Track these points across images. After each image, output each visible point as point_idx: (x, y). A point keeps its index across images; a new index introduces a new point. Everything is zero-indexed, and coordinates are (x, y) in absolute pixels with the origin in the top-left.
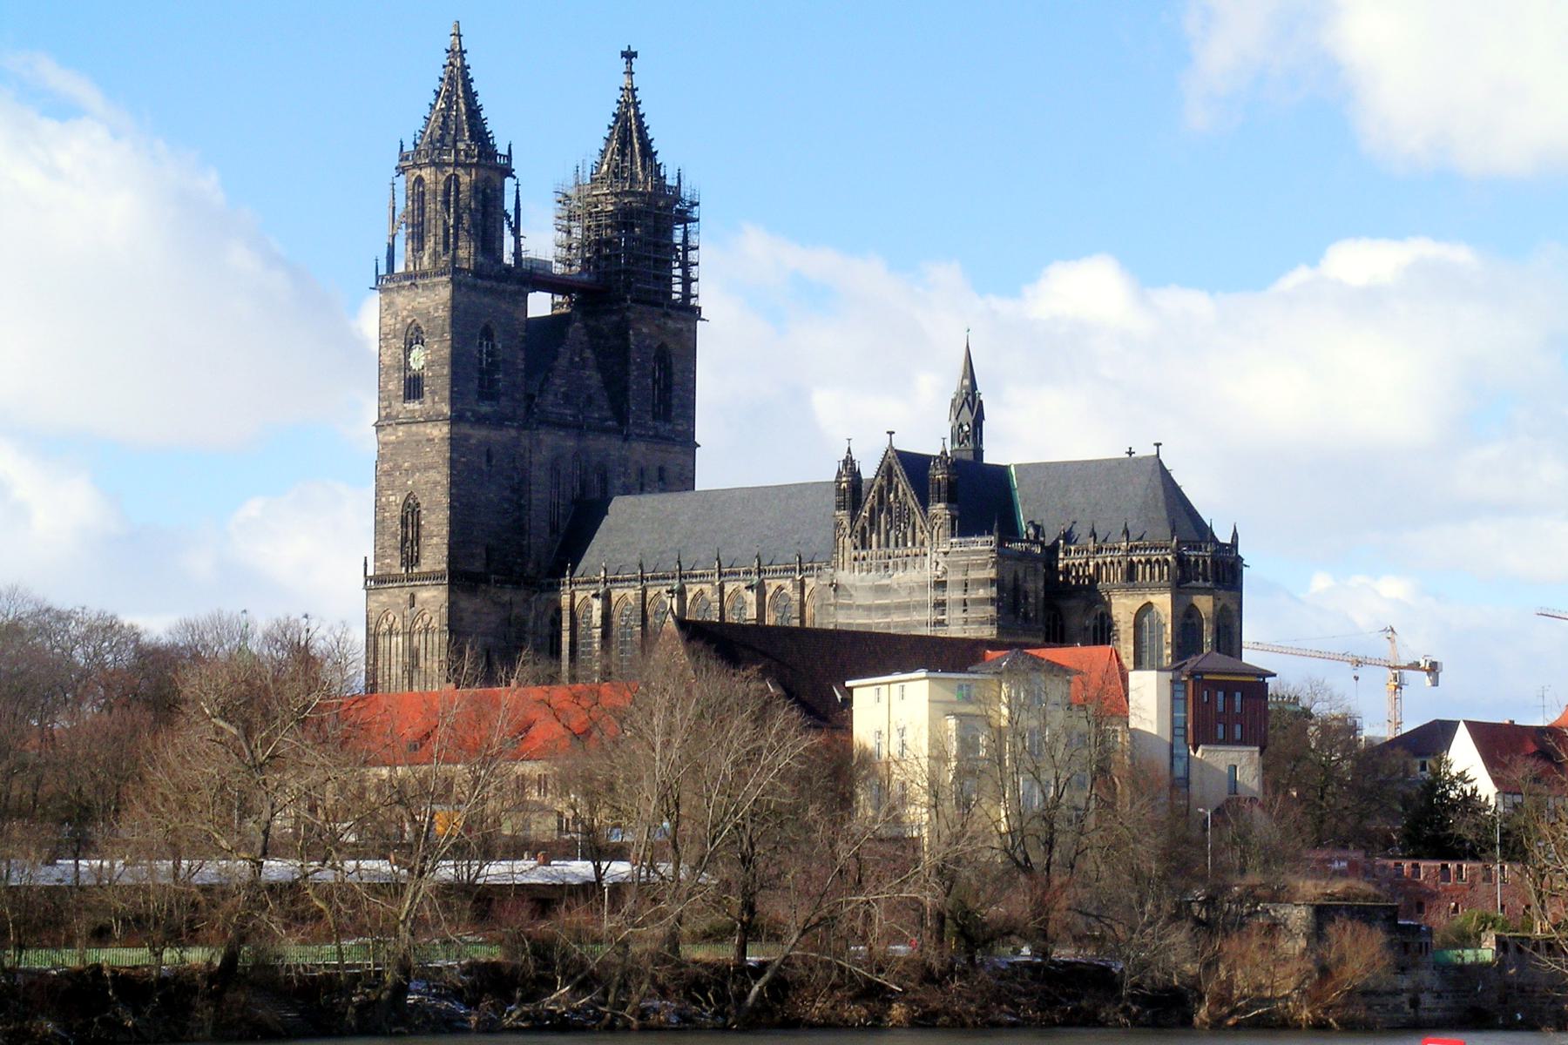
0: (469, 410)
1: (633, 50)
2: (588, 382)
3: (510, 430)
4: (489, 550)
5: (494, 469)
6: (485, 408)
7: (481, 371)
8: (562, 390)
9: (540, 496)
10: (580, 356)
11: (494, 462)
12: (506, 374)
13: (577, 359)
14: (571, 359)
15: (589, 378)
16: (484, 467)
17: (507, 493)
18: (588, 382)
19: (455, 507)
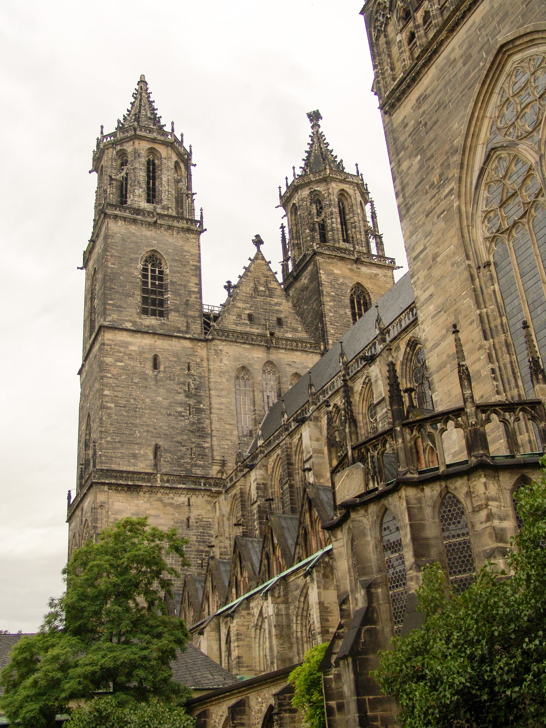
0: (130, 321)
1: (315, 109)
2: (277, 308)
3: (182, 341)
4: (157, 448)
5: (162, 375)
6: (151, 321)
7: (145, 291)
8: (247, 312)
9: (223, 400)
10: (266, 286)
11: (162, 368)
12: (176, 293)
13: (262, 288)
14: (256, 289)
15: (279, 304)
16: (149, 371)
17: (181, 397)
18: (277, 308)
19: (110, 408)
